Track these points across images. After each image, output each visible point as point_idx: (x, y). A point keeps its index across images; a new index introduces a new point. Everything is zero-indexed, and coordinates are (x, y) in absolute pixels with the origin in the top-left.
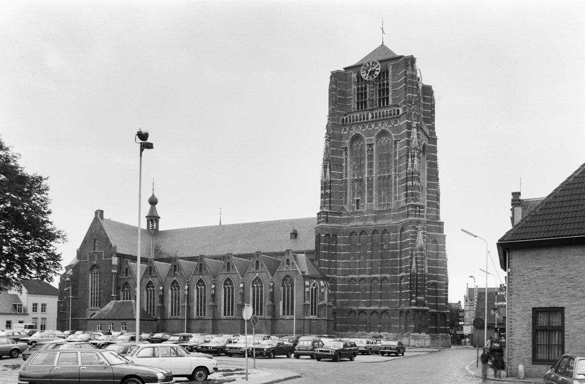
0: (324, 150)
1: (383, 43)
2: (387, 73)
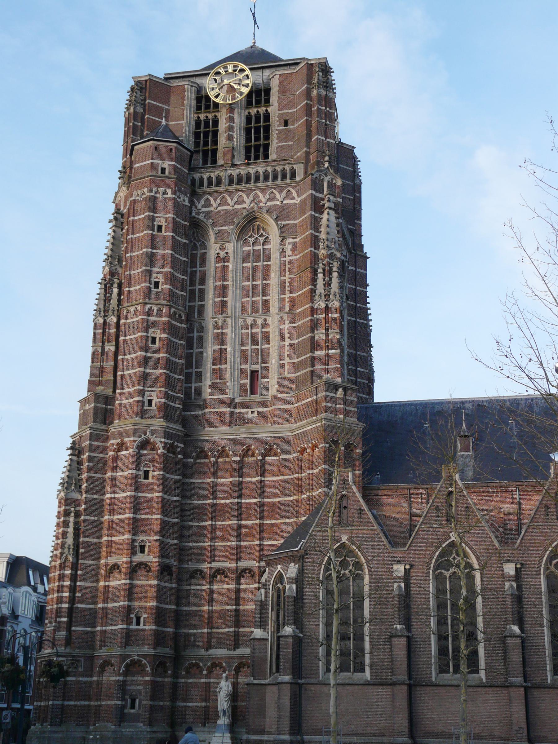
0: (108, 244)
1: (255, 43)
2: (268, 91)
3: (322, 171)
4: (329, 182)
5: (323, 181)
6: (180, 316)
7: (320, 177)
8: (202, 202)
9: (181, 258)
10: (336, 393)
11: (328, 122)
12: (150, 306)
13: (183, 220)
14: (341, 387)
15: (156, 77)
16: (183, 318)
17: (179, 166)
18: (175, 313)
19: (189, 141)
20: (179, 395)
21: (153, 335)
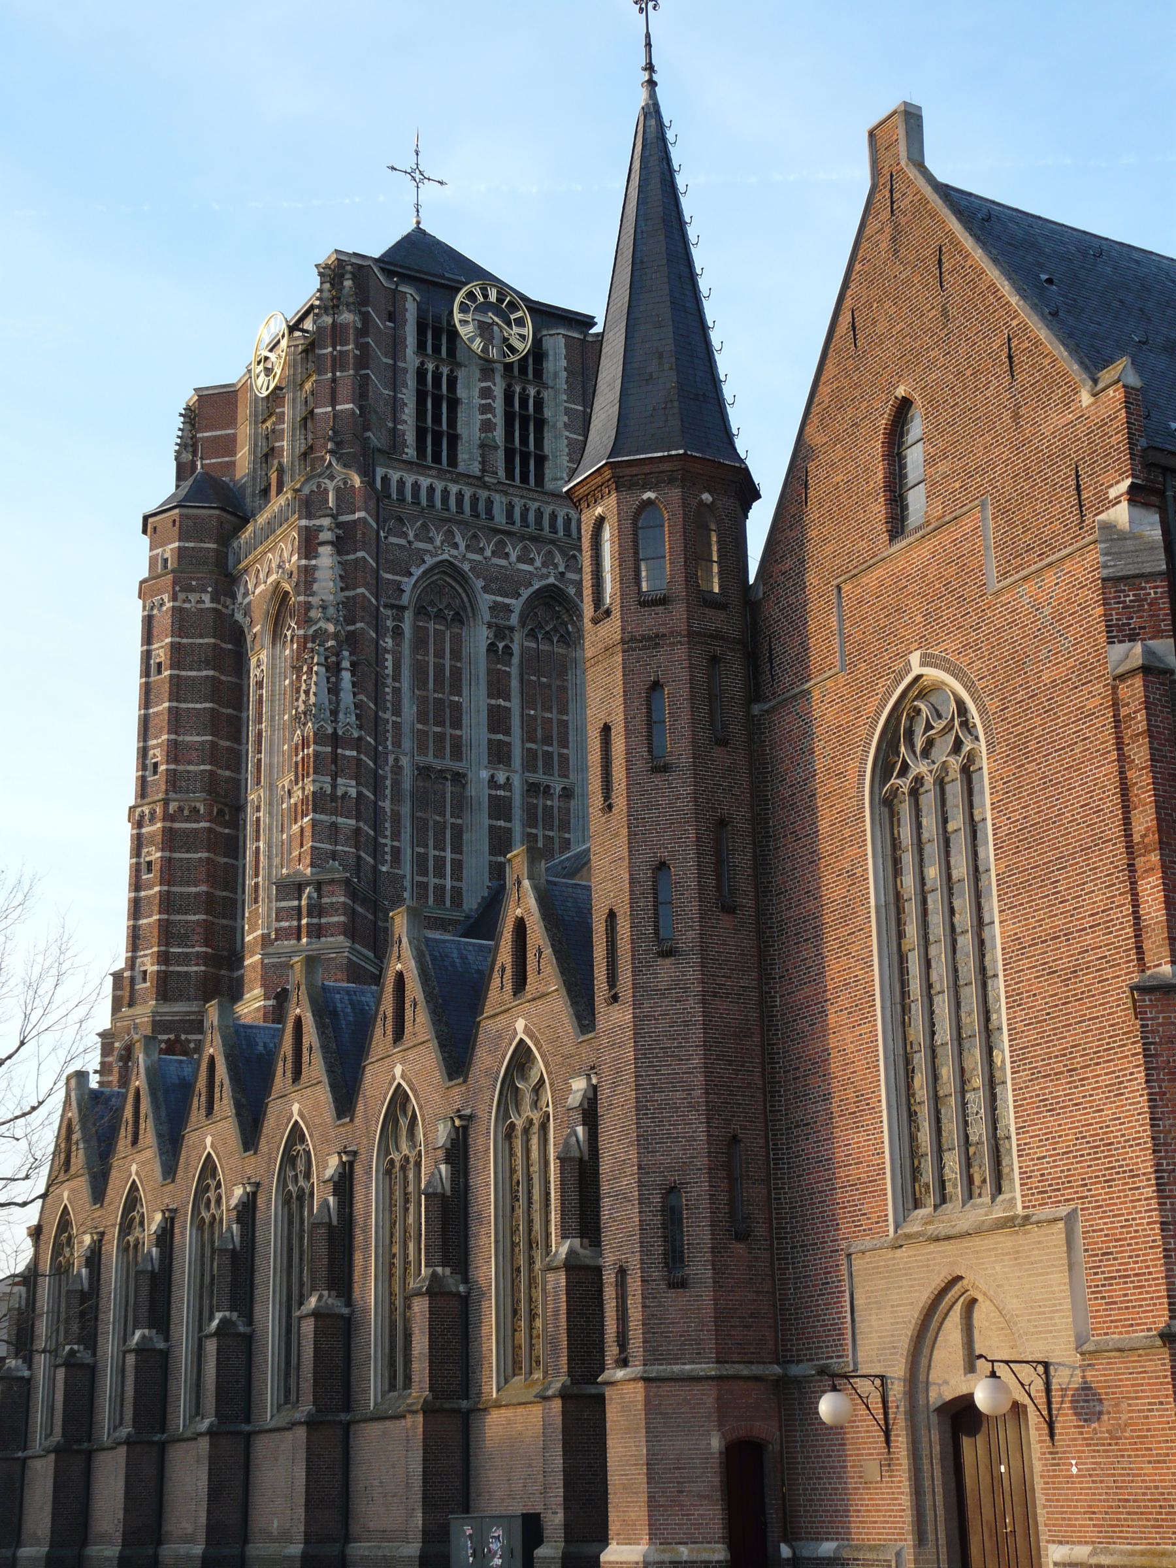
3: (320, 475)
4: (338, 490)
5: (326, 491)
6: (195, 810)
7: (319, 486)
8: (242, 590)
9: (198, 706)
10: (300, 899)
11: (338, 374)
12: (139, 809)
13: (201, 637)
14: (308, 884)
15: (207, 388)
16: (202, 812)
17: (192, 545)
18: (181, 809)
19: (254, 479)
20: (197, 949)
21: (148, 859)
